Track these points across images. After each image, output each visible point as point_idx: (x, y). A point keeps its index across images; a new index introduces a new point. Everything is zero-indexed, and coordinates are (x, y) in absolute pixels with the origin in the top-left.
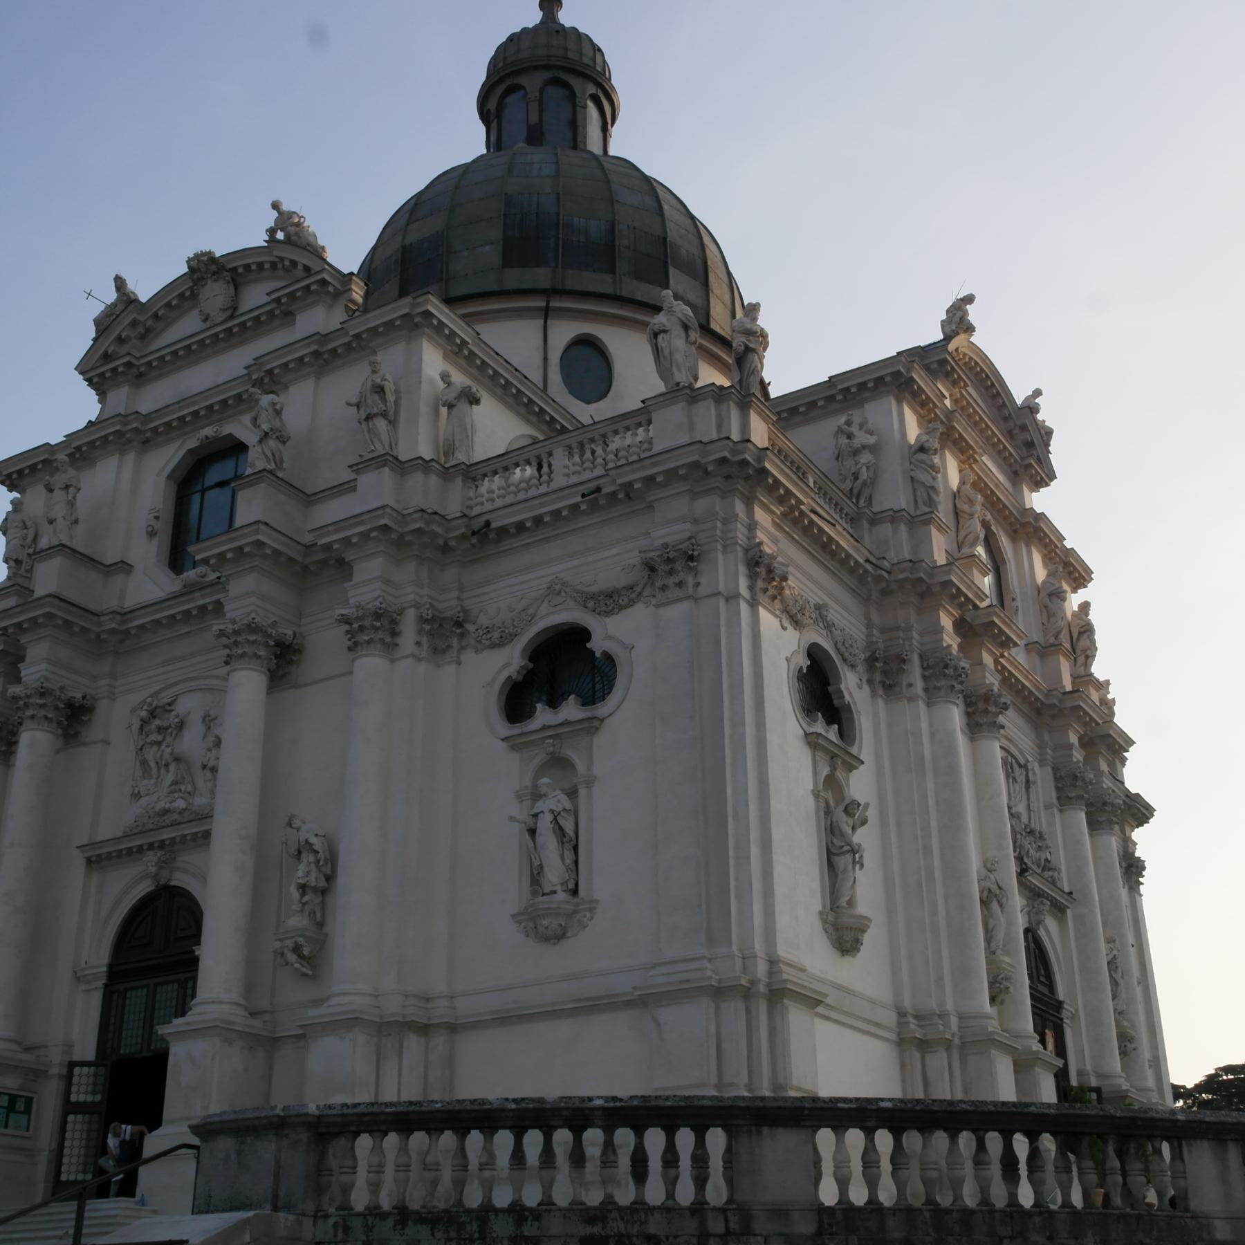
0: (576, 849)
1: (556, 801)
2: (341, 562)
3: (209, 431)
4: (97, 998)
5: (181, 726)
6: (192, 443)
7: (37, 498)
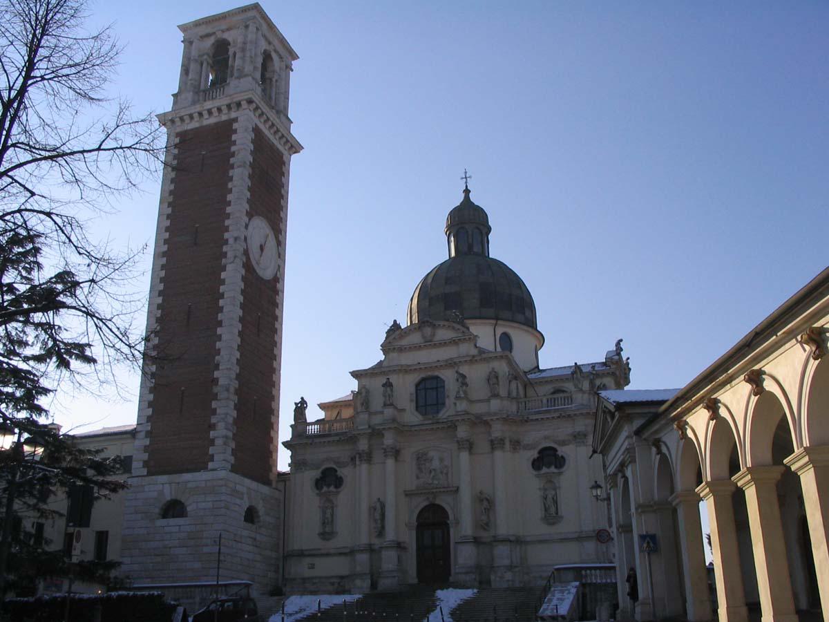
0: (557, 504)
1: (550, 494)
2: (488, 423)
3: (430, 373)
4: (414, 533)
5: (431, 460)
6: (423, 375)
7: (366, 381)
